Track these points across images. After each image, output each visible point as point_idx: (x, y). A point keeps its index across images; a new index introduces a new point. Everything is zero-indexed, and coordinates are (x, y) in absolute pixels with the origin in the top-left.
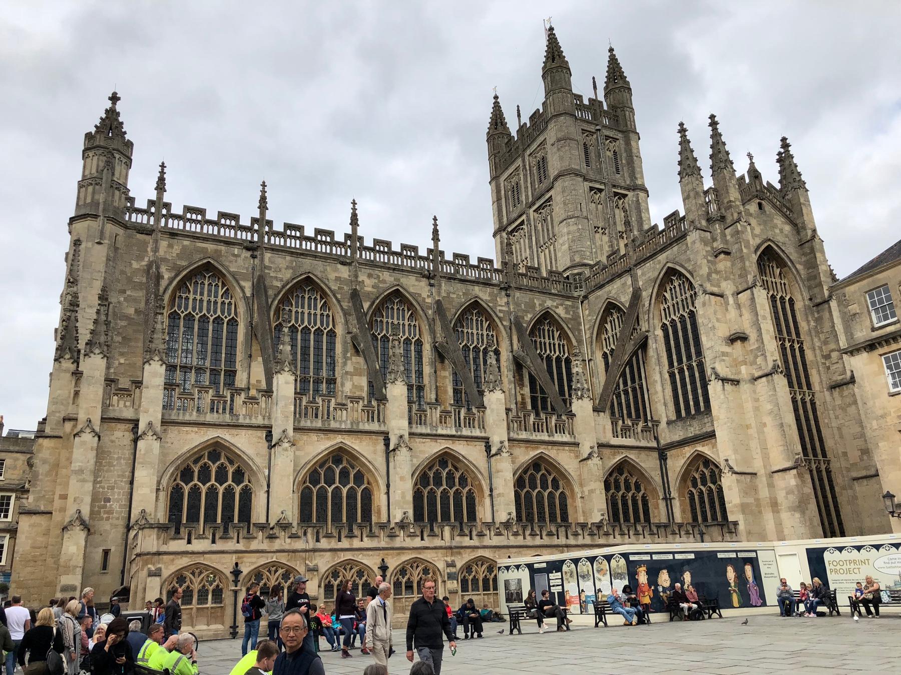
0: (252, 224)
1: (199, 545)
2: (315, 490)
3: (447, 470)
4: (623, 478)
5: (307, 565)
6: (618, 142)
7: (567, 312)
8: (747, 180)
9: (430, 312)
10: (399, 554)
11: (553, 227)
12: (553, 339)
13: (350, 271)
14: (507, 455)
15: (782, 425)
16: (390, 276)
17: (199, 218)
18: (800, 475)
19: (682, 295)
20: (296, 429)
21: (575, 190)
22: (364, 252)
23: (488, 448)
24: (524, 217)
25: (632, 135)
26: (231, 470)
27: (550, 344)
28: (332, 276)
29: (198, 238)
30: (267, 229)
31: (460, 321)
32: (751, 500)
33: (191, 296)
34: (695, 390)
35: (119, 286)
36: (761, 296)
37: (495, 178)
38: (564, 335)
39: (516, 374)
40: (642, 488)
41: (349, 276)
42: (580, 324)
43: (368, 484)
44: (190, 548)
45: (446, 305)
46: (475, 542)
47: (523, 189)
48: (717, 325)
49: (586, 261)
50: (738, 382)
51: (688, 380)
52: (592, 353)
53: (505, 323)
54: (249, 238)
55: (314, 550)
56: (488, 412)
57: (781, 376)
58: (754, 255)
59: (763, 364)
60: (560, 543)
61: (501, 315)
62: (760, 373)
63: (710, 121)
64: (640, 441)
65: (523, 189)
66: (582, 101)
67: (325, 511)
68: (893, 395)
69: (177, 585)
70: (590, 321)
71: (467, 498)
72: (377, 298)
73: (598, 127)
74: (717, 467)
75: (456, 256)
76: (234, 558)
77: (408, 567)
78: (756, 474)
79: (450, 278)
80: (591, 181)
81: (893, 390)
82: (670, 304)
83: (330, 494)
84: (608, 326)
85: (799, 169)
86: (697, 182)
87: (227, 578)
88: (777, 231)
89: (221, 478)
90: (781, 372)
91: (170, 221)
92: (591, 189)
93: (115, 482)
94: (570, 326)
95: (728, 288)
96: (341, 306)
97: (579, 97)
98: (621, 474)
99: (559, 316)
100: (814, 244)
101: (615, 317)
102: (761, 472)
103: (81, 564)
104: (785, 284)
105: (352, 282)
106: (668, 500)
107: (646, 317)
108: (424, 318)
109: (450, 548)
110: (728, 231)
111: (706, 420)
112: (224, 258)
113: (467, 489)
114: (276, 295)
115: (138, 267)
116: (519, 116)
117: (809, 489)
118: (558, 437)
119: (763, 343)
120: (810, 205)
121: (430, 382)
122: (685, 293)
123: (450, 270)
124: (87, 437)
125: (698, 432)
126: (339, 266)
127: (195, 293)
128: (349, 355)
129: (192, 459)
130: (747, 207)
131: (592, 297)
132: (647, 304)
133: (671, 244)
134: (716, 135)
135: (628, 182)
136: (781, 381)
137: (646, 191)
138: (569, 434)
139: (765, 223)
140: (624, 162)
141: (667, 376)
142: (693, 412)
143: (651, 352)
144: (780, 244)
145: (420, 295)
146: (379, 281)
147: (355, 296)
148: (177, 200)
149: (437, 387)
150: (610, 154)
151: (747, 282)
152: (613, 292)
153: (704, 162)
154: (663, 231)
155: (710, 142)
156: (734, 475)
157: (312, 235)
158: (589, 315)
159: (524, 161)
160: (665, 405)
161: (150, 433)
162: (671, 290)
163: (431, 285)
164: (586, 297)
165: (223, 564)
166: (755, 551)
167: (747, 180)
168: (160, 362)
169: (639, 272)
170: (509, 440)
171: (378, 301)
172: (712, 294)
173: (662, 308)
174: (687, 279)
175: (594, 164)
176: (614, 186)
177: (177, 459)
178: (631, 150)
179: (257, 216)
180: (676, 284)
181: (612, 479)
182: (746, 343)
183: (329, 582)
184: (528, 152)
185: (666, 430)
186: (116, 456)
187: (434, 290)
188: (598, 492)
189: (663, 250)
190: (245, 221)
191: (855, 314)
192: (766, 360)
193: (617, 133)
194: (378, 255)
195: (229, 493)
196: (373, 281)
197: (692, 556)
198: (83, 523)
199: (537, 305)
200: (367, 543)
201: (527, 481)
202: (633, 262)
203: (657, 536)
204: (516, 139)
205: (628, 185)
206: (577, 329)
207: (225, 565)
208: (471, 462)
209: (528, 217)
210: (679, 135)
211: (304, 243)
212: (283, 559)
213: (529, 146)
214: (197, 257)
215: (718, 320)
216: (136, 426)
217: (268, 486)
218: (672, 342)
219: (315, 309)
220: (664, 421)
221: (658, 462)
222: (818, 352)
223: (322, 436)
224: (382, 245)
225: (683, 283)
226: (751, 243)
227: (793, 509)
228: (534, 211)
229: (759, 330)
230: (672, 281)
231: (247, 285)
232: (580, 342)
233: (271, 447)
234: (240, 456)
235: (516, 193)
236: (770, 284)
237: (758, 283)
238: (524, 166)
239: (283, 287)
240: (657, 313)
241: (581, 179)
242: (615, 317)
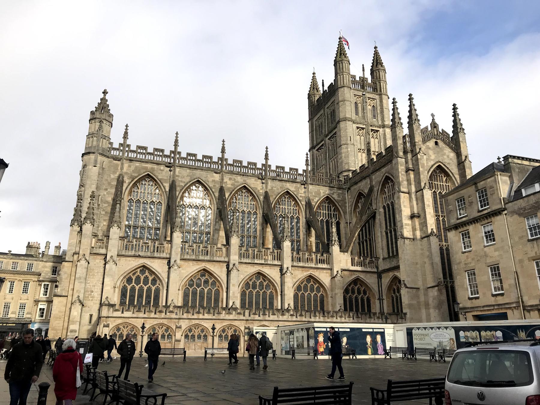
0: (171, 154)
1: (127, 314)
2: (191, 290)
3: (259, 281)
4: (356, 288)
5: (176, 325)
7: (339, 195)
8: (429, 129)
9: (262, 198)
10: (222, 322)
12: (331, 211)
14: (290, 274)
15: (432, 263)
16: (241, 179)
17: (144, 151)
18: (439, 290)
20: (181, 259)
21: (347, 129)
22: (228, 167)
23: (281, 270)
24: (323, 142)
25: (384, 96)
26: (150, 278)
27: (328, 214)
28: (210, 179)
29: (143, 162)
30: (178, 156)
31: (278, 202)
32: (414, 302)
33: (139, 191)
34: (392, 244)
35: (104, 187)
36: (428, 194)
37: (311, 120)
38: (336, 209)
39: (307, 230)
40: (368, 293)
43: (218, 287)
44: (123, 315)
45: (270, 193)
46: (261, 318)
48: (403, 208)
49: (351, 169)
51: (393, 237)
52: (351, 219)
53: (303, 203)
54: (169, 161)
55: (180, 319)
56: (282, 251)
57: (435, 237)
58: (426, 172)
59: (426, 230)
60: (306, 320)
61: (301, 198)
64: (367, 268)
66: (355, 79)
67: (196, 300)
68: (463, 253)
69: (117, 332)
70: (351, 201)
71: (269, 295)
72: (233, 190)
75: (277, 167)
76: (142, 321)
77: (226, 328)
78: (419, 288)
79: (273, 179)
80: (358, 123)
81: (464, 250)
82: (387, 194)
83: (198, 292)
84: (360, 205)
85: (461, 122)
86: (400, 131)
87: (139, 330)
88: (445, 157)
89: (146, 281)
90: (435, 235)
91: (130, 154)
92: (358, 128)
93: (96, 283)
94: (340, 204)
96: (214, 195)
97: (354, 77)
98: (356, 286)
99: (334, 199)
100: (465, 164)
102: (421, 288)
103: (79, 320)
104: (448, 186)
106: (381, 299)
108: (258, 201)
109: (247, 320)
110: (414, 158)
112: (156, 172)
113: (270, 291)
114: (181, 190)
115: (114, 177)
116: (323, 86)
117: (444, 297)
118: (320, 266)
120: (466, 142)
121: (260, 234)
123: (273, 175)
124: (83, 262)
125: (396, 265)
126: (215, 174)
127: (141, 189)
129: (132, 273)
130: (428, 144)
131: (352, 188)
133: (387, 163)
135: (380, 123)
138: (327, 264)
139: (438, 153)
140: (378, 112)
141: (384, 234)
143: (377, 221)
144: (446, 164)
145: (256, 188)
146: (235, 182)
147: (222, 190)
148: (133, 142)
149: (263, 236)
152: (362, 187)
153: (405, 120)
154: (385, 156)
155: (408, 109)
156: (407, 289)
157: (201, 158)
158: (350, 199)
159: (324, 111)
160: (382, 249)
161: (112, 261)
163: (263, 183)
164: (349, 189)
165: (137, 323)
166: (384, 329)
167: (429, 129)
168: (117, 227)
169: (373, 177)
170: (292, 266)
171: (234, 192)
175: (360, 114)
176: (371, 126)
177: (124, 273)
178: (383, 105)
179: (173, 149)
180: (390, 184)
181: (350, 288)
183: (187, 334)
184: (327, 106)
185: (382, 263)
186: (96, 271)
187: (264, 185)
188: (339, 295)
189: (384, 166)
190: (167, 153)
194: (235, 168)
195: (149, 290)
196: (232, 182)
197: (349, 330)
198: (80, 301)
199: (322, 193)
200: (206, 316)
201: (302, 288)
202: (371, 171)
203: (360, 319)
205: (380, 125)
207: (138, 323)
208: (271, 278)
211: (197, 163)
212: (165, 322)
213: (327, 103)
214: (142, 171)
215: (404, 206)
216: (106, 257)
217: (168, 287)
218: (387, 216)
220: (381, 257)
221: (377, 279)
223: (195, 263)
226: (425, 165)
227: (435, 308)
228: (328, 139)
230: (388, 183)
231: (167, 186)
233: (169, 268)
234: (154, 272)
236: (439, 186)
237: (426, 187)
238: (325, 114)
239: (185, 186)
240: (381, 199)
241: (352, 123)
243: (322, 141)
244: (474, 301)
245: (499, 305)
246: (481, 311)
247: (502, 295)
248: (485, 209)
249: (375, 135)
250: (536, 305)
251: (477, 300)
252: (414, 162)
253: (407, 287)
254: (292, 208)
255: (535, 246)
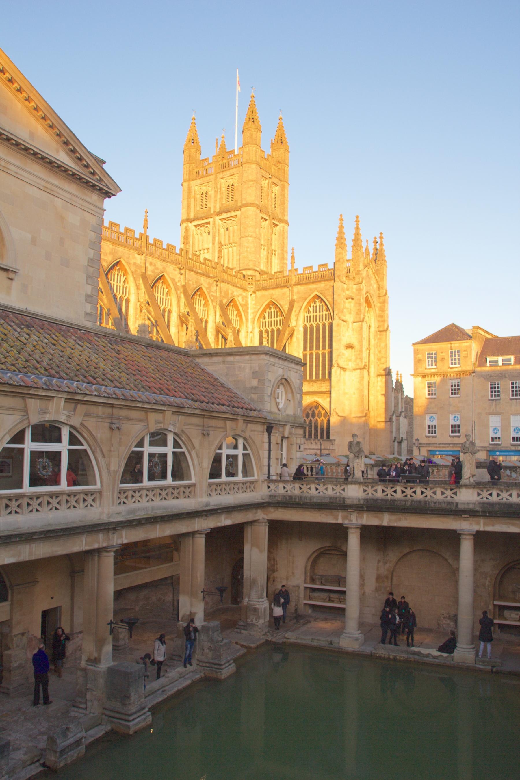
6: (278, 187)
11: (233, 236)
13: (141, 259)
19: (320, 312)
24: (210, 220)
25: (286, 185)
28: (132, 262)
38: (239, 315)
41: (141, 263)
42: (248, 308)
47: (213, 201)
50: (346, 369)
52: (253, 328)
61: (212, 298)
62: (357, 367)
63: (356, 219)
65: (213, 201)
70: (255, 308)
73: (270, 176)
74: (323, 409)
84: (266, 315)
88: (371, 288)
92: (262, 218)
95: (350, 318)
99: (239, 303)
101: (273, 310)
105: (141, 267)
107: (295, 318)
108: (175, 296)
110: (355, 287)
111: (323, 385)
119: (362, 352)
122: (322, 312)
125: (316, 390)
126: (137, 255)
128: (137, 316)
132: (298, 311)
134: (357, 228)
136: (365, 372)
137: (288, 225)
142: (314, 378)
143: (294, 339)
145: (174, 280)
147: (144, 277)
150: (273, 194)
151: (360, 318)
153: (349, 242)
155: (354, 231)
158: (255, 304)
162: (313, 307)
172: (343, 321)
173: (306, 315)
174: (326, 304)
178: (284, 195)
182: (353, 350)
184: (220, 175)
187: (182, 277)
191: (420, 360)
192: (362, 362)
193: (278, 181)
199: (230, 294)
204: (211, 161)
206: (246, 312)
209: (214, 221)
210: (339, 222)
219: (120, 283)
222: (376, 356)
224: (157, 243)
225: (322, 306)
229: (361, 346)
232: (247, 320)
235: (204, 199)
242: (273, 310)
243: (208, 218)
244: (431, 439)
245: (454, 444)
246: (436, 447)
247: (459, 437)
248: (456, 367)
249: (274, 229)
250: (485, 447)
251: (434, 439)
252: (354, 290)
253: (339, 416)
254: (202, 308)
255: (494, 404)
